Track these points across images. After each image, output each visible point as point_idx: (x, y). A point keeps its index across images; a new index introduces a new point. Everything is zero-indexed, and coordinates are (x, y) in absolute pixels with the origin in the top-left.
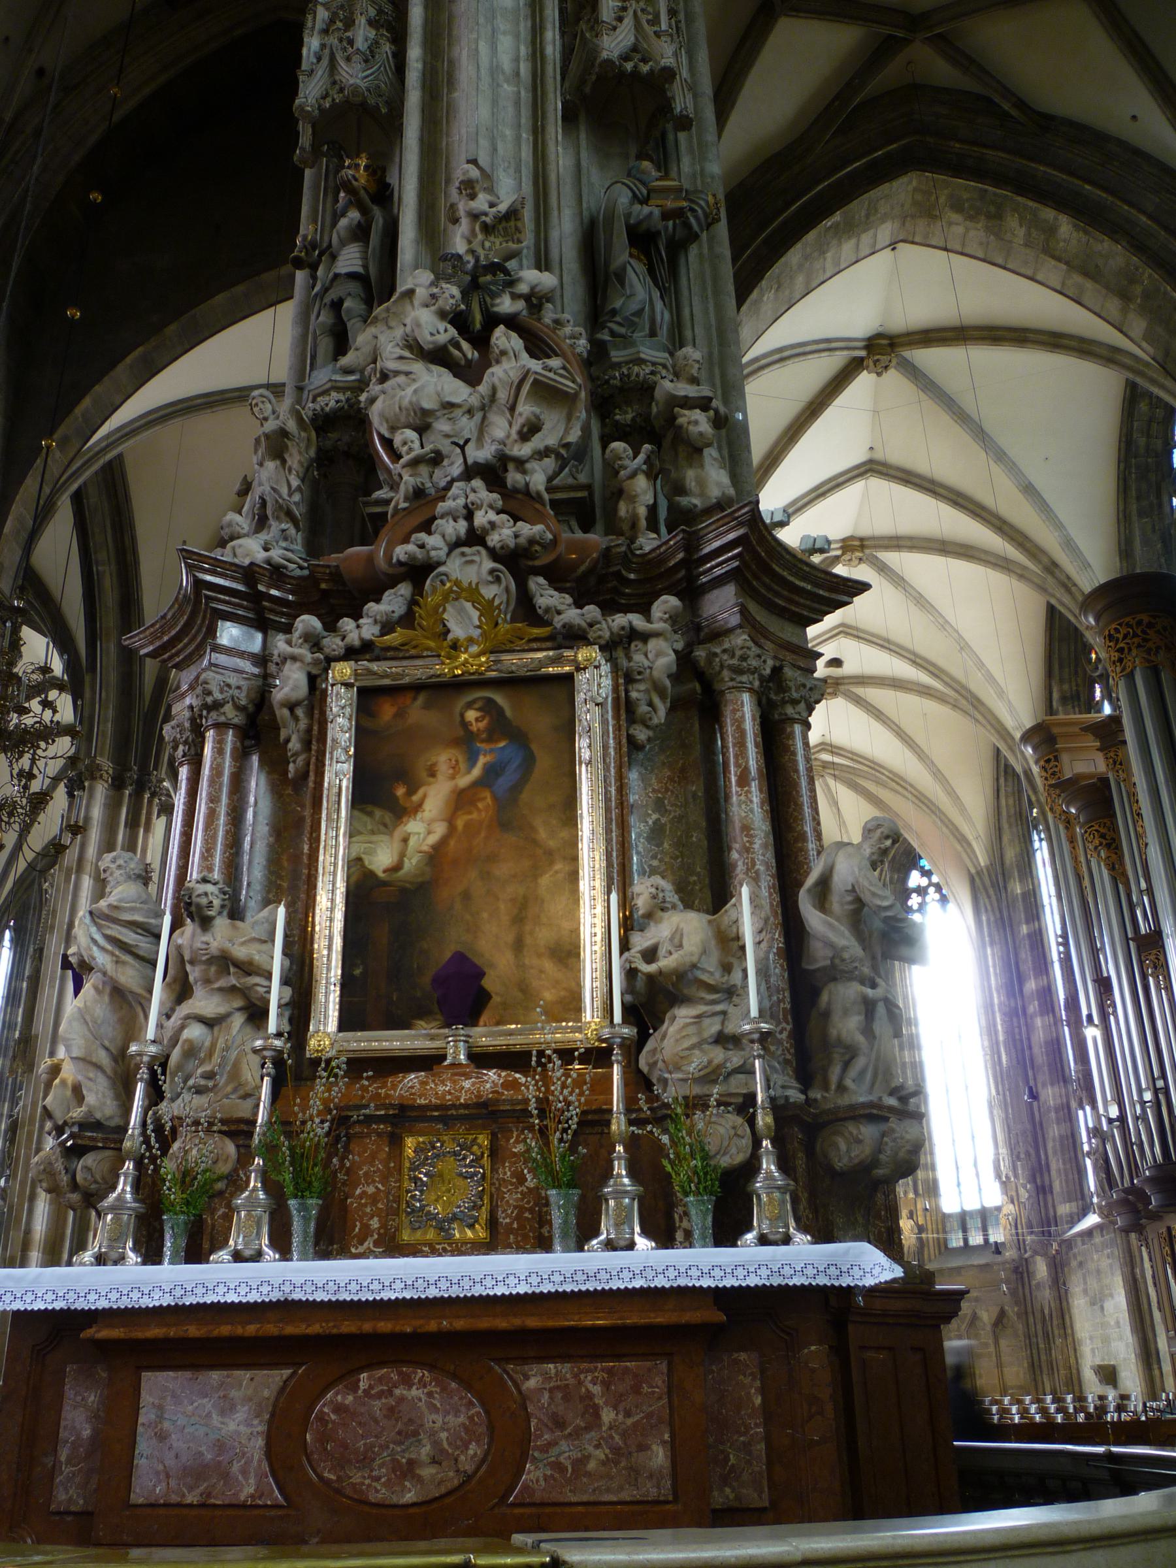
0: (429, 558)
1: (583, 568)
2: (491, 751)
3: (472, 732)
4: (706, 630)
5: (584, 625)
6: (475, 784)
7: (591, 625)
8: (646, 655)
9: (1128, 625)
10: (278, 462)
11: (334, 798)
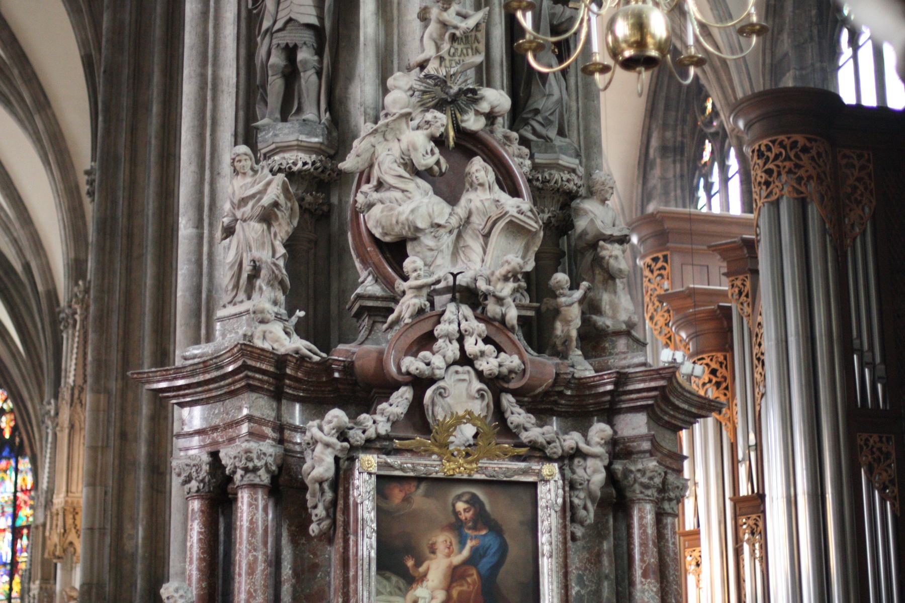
0: (433, 374)
1: (540, 390)
2: (476, 537)
3: (461, 521)
4: (621, 446)
5: (544, 442)
6: (468, 562)
7: (549, 443)
8: (585, 469)
9: (781, 144)
10: (265, 227)
11: (366, 566)
